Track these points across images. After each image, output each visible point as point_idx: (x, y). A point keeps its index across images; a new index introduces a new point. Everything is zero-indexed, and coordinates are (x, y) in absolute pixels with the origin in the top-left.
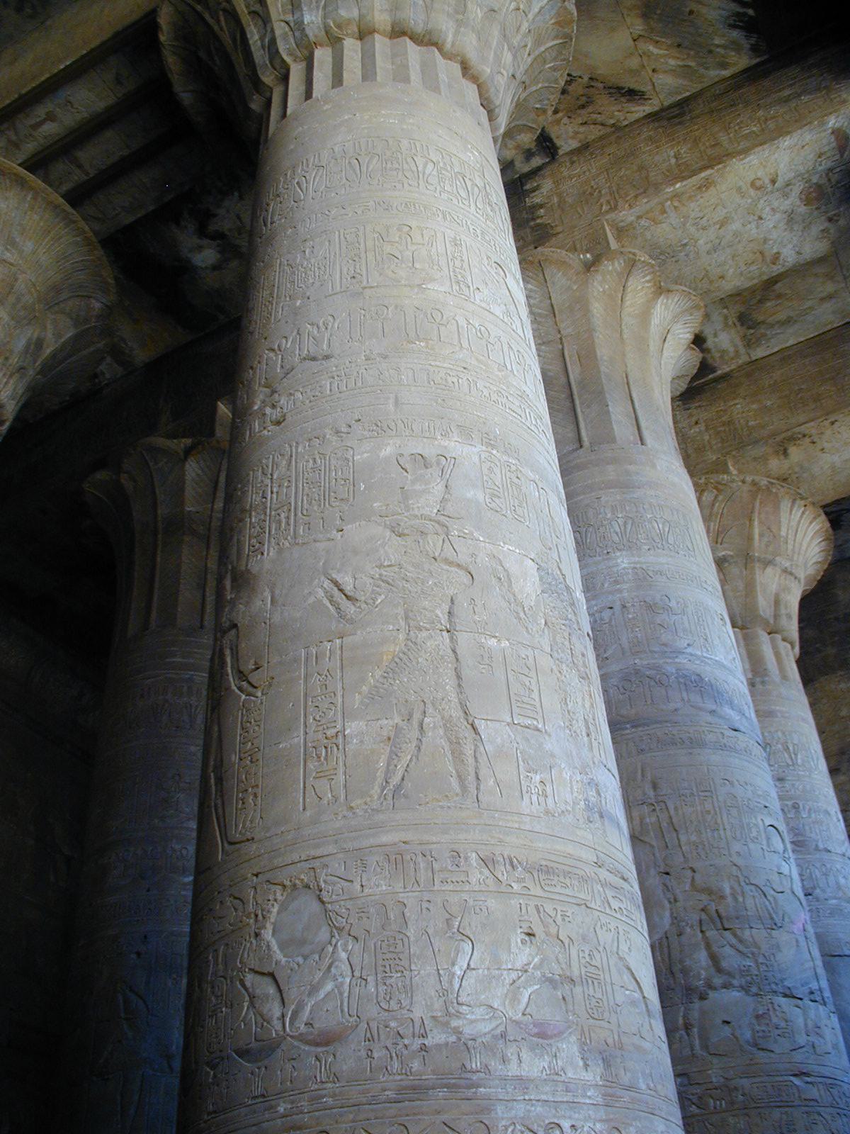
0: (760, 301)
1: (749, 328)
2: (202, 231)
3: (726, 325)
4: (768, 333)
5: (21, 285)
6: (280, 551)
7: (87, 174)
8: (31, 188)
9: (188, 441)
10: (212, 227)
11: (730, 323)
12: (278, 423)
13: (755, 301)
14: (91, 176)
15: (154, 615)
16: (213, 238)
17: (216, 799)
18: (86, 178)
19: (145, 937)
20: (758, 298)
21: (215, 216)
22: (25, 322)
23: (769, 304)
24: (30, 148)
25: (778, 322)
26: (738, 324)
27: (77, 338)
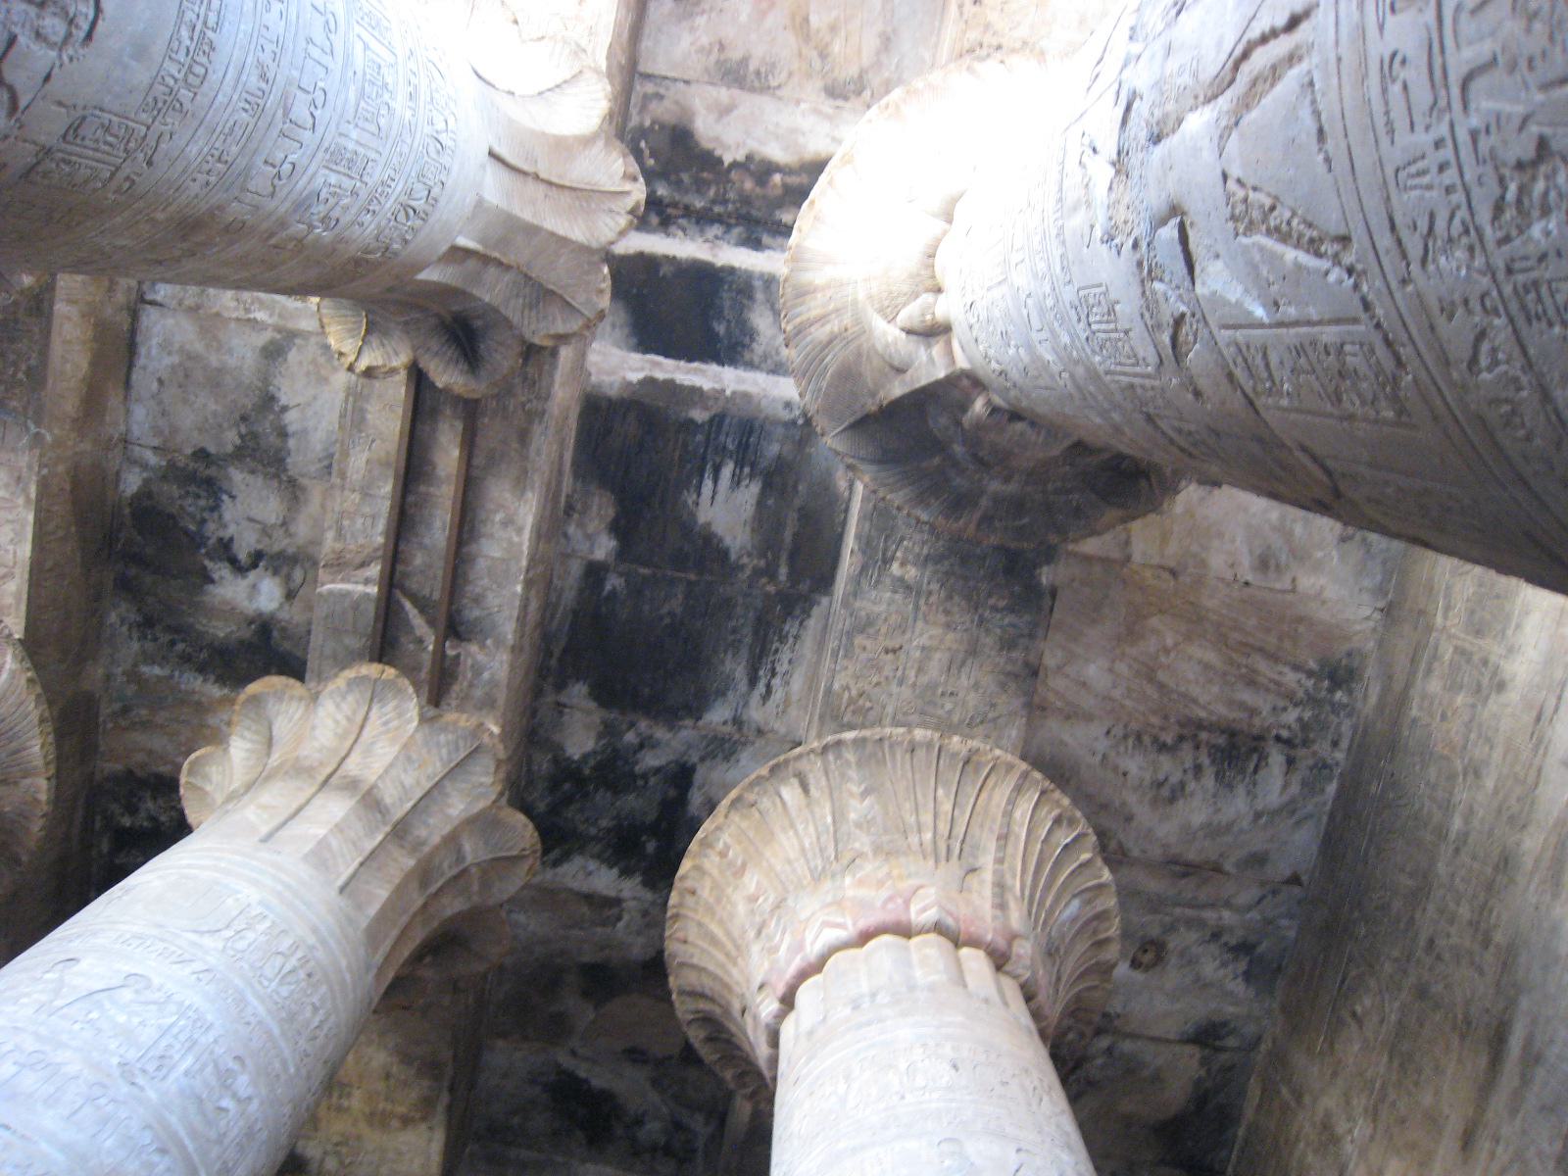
0: (823, 55)
1: (859, 93)
3: (829, 118)
4: (887, 74)
10: (243, 556)
11: (830, 111)
13: (817, 64)
16: (255, 566)
20: (815, 54)
21: (231, 539)
23: (837, 47)
25: (878, 53)
26: (840, 103)
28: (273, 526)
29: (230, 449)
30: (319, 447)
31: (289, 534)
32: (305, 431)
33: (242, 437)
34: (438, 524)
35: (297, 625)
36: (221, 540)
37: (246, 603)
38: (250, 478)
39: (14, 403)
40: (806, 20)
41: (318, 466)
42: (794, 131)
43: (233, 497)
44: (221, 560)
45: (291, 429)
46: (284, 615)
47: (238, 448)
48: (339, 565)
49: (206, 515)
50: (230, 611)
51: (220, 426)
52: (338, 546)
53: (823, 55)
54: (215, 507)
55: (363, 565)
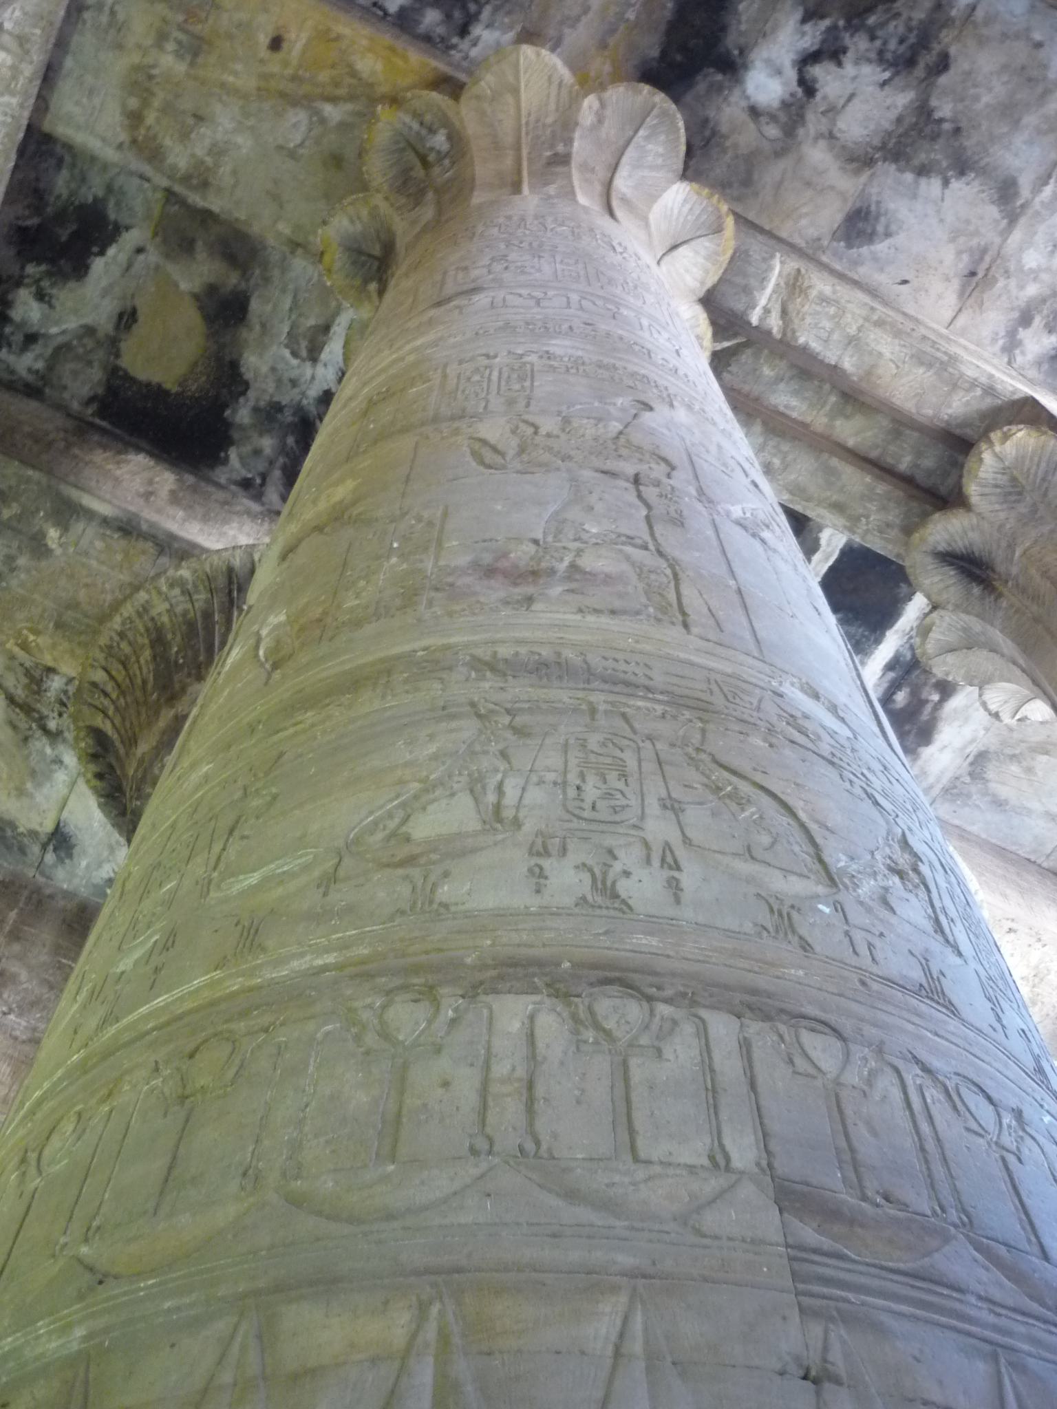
1: (970, 774)
2: (809, 59)
4: (975, 797)
10: (817, 71)
11: (968, 751)
13: (1009, 751)
16: (802, 81)
20: (1017, 752)
21: (839, 64)
23: (1014, 768)
25: (994, 795)
26: (971, 759)
28: (833, 122)
29: (934, 102)
30: (892, 206)
31: (819, 136)
33: (941, 120)
34: (794, 402)
35: (719, 109)
36: (844, 50)
37: (765, 54)
38: (893, 114)
40: (1047, 753)
41: (874, 198)
42: (966, 720)
43: (884, 84)
44: (823, 41)
45: (923, 181)
46: (735, 96)
47: (929, 113)
48: (794, 286)
49: (878, 43)
50: (763, 33)
51: (962, 100)
52: (813, 293)
53: (1013, 757)
54: (881, 58)
55: (784, 313)
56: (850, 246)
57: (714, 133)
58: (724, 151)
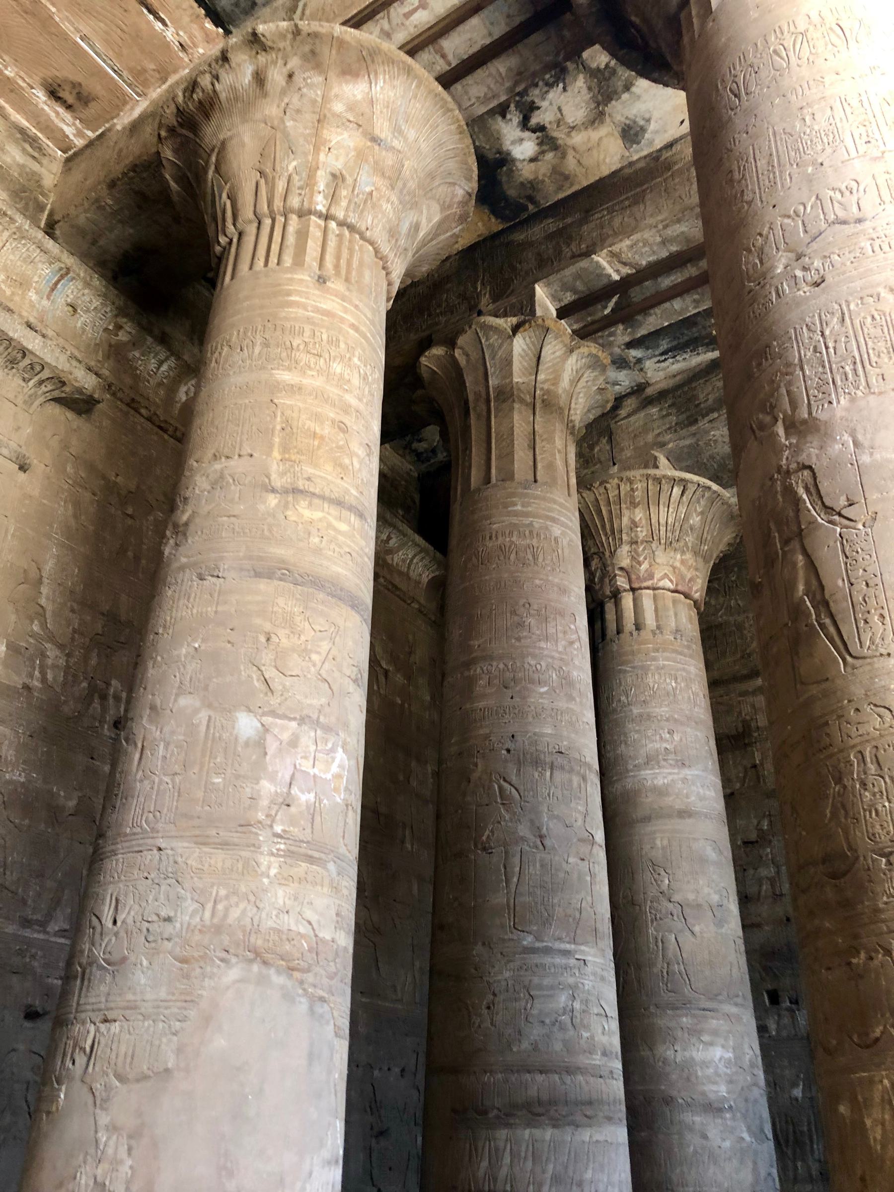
2: (525, 124)
5: (406, 172)
6: (853, 400)
7: (450, 64)
8: (416, 77)
9: (514, 320)
10: (534, 121)
12: (817, 284)
14: (453, 65)
15: (493, 471)
17: (818, 616)
18: (448, 68)
19: (513, 736)
21: (538, 108)
22: (409, 206)
24: (401, 37)
27: (440, 224)
28: (566, 123)
29: (594, 65)
30: (634, 111)
31: (568, 134)
32: (639, 97)
33: (607, 65)
34: (673, 278)
35: (520, 175)
36: (533, 102)
37: (508, 143)
38: (585, 90)
39: (567, 33)
41: (623, 119)
43: (565, 89)
44: (521, 112)
45: (633, 89)
47: (598, 69)
48: (615, 256)
50: (498, 138)
55: (625, 264)
56: (638, 143)
57: (530, 182)
58: (543, 181)
